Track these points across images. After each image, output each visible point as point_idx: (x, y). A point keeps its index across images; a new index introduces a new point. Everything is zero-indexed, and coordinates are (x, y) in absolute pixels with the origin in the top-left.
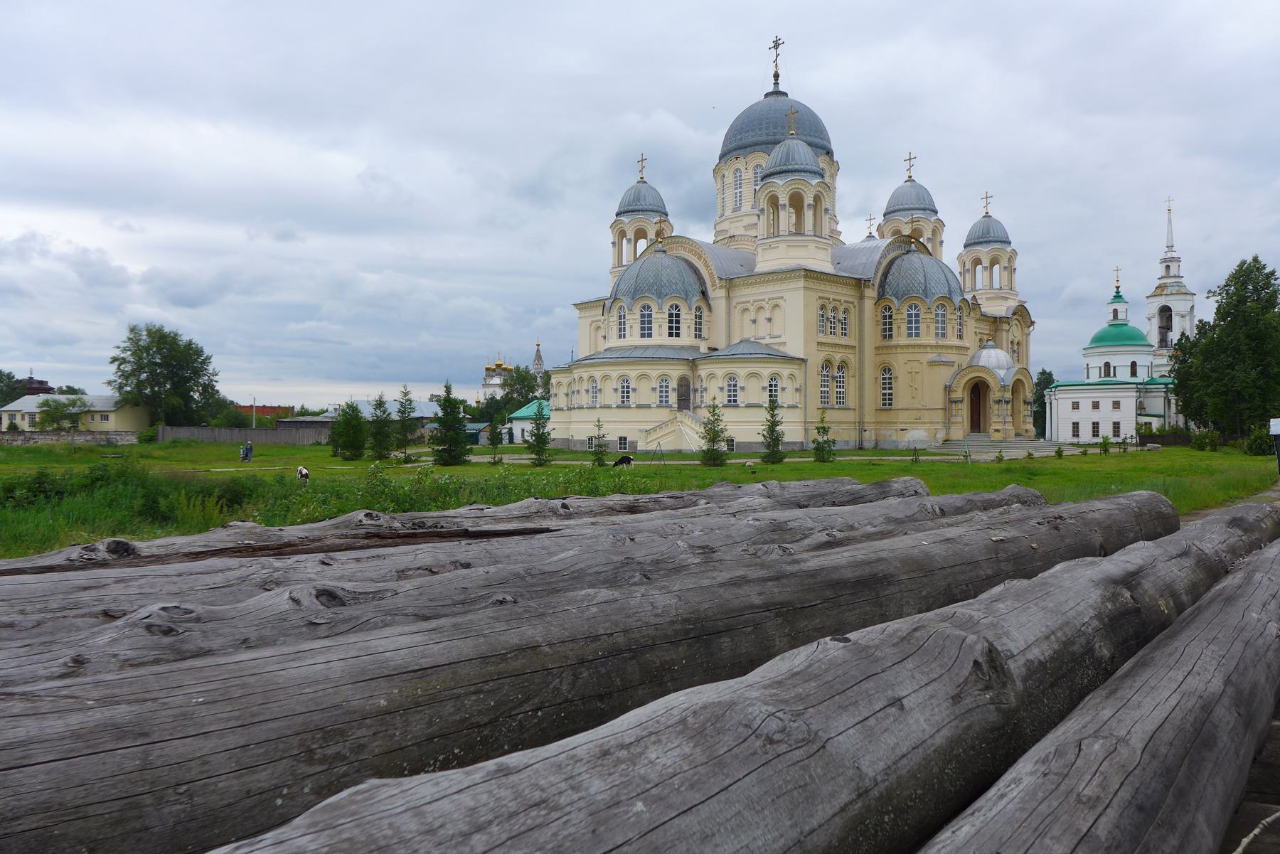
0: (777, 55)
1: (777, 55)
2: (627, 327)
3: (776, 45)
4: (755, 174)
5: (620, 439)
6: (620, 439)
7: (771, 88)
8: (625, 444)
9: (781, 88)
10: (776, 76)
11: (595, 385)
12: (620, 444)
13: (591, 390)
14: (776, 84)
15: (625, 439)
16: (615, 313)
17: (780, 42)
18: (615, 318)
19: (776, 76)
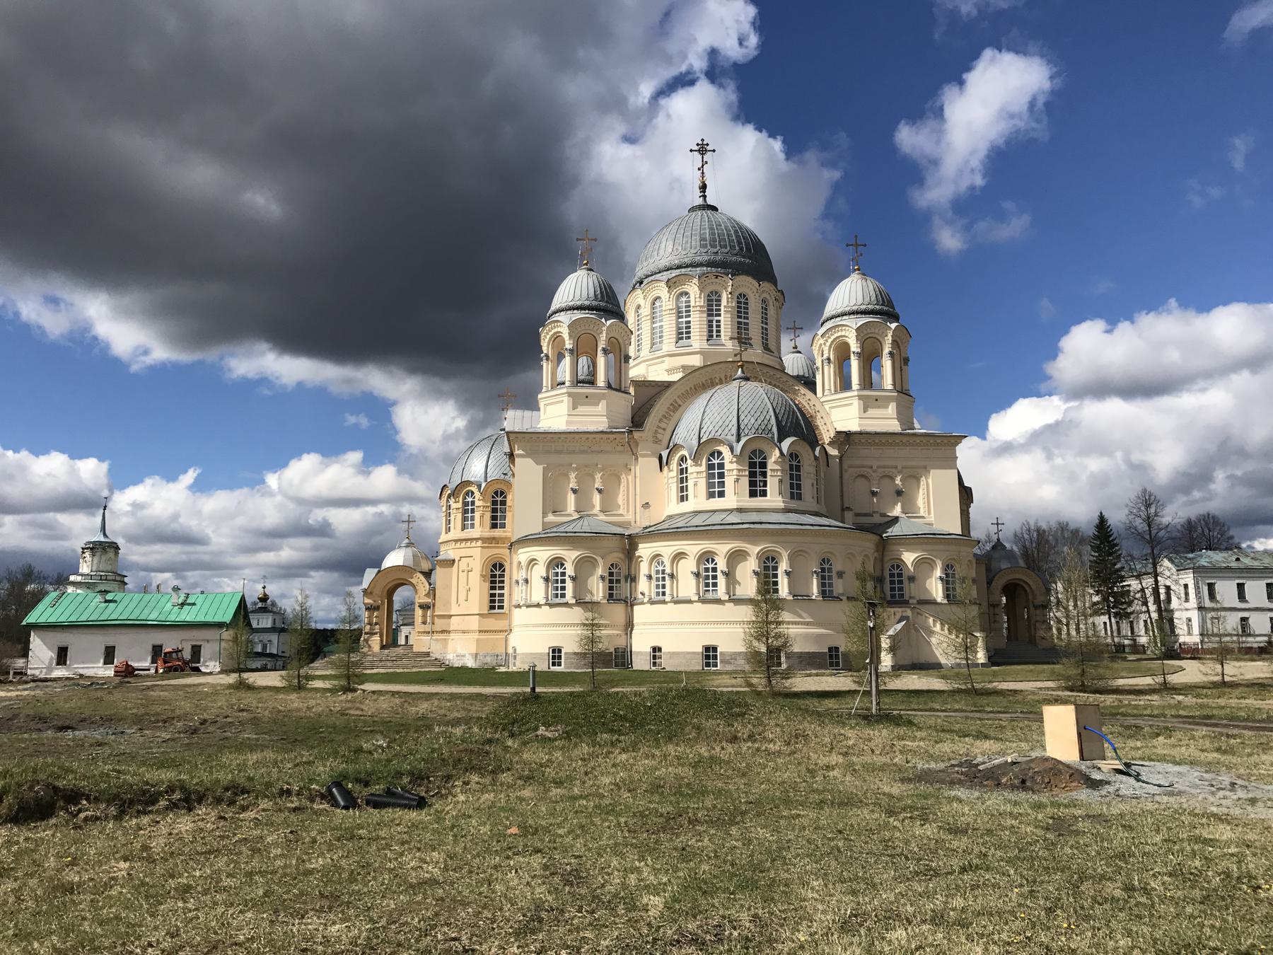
0: (704, 163)
1: (704, 163)
2: (690, 484)
3: (702, 149)
4: (708, 300)
5: (830, 649)
6: (830, 649)
7: (700, 201)
8: (837, 657)
9: (710, 201)
10: (703, 187)
11: (660, 568)
12: (831, 656)
13: (654, 576)
14: (705, 197)
15: (715, 649)
16: (674, 464)
17: (708, 148)
18: (672, 473)
19: (703, 187)
